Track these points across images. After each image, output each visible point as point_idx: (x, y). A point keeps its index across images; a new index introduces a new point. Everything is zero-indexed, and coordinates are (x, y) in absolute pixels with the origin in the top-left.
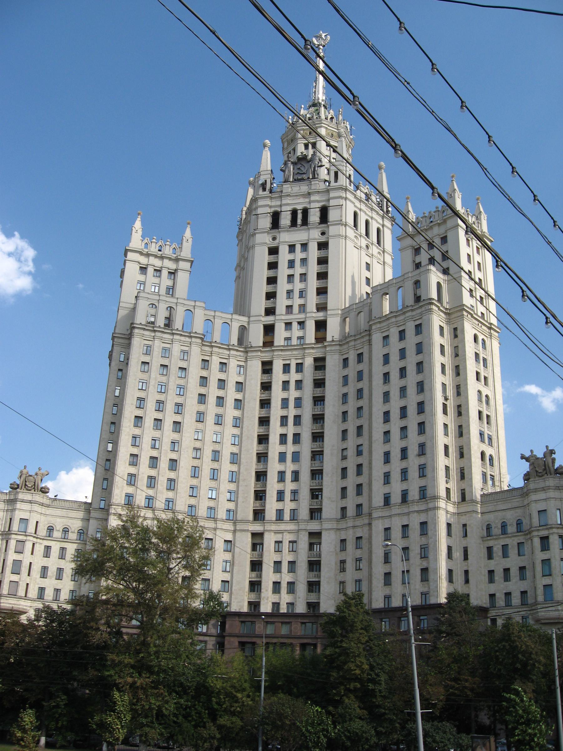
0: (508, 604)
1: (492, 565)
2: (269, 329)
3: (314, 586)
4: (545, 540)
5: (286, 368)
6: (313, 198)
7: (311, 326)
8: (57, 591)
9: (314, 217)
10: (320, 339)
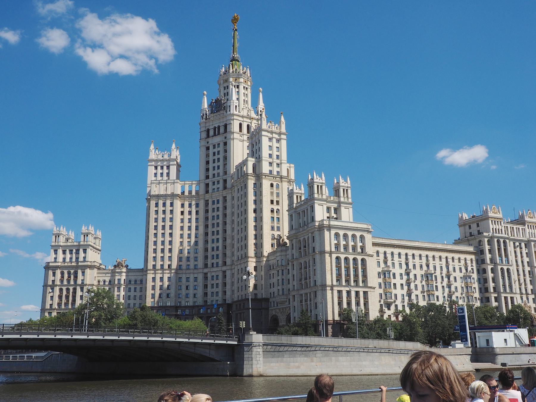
2: (207, 185)
5: (213, 202)
6: (222, 120)
9: (222, 130)
10: (225, 188)
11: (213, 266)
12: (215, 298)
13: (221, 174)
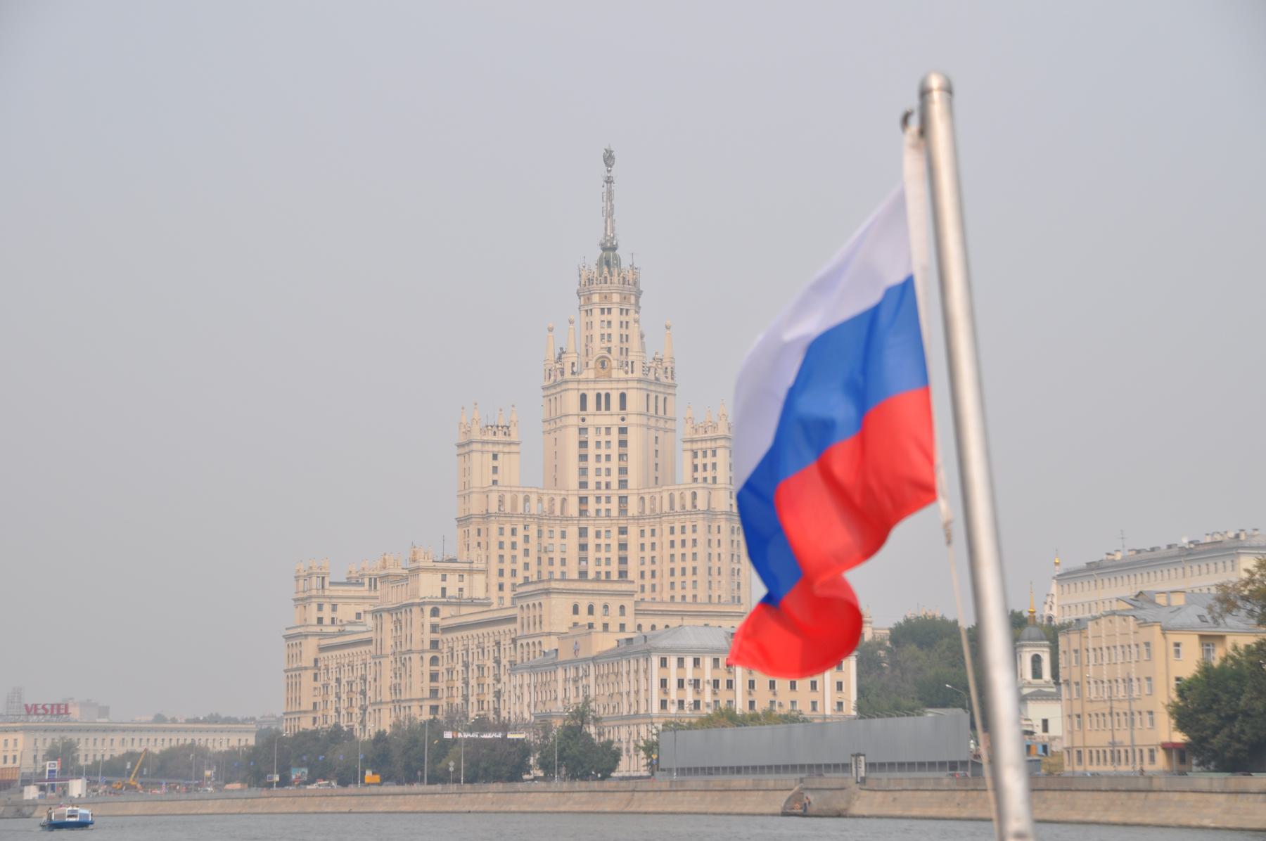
2: (583, 500)
5: (598, 535)
6: (614, 385)
7: (615, 500)
10: (623, 511)
13: (615, 485)
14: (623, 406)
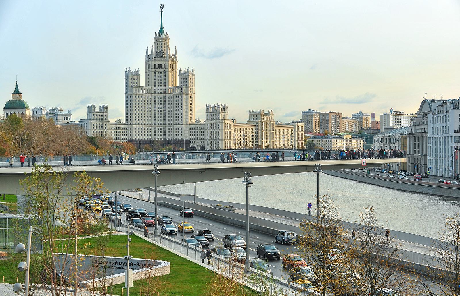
0: (193, 139)
1: (191, 134)
3: (164, 135)
4: (197, 131)
5: (159, 98)
7: (163, 90)
8: (125, 138)
9: (163, 67)
10: (165, 92)
11: (159, 124)
12: (160, 137)
13: (163, 86)
14: (165, 67)
